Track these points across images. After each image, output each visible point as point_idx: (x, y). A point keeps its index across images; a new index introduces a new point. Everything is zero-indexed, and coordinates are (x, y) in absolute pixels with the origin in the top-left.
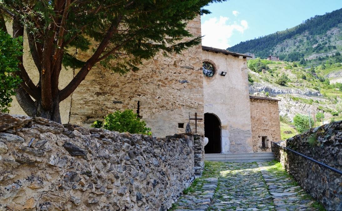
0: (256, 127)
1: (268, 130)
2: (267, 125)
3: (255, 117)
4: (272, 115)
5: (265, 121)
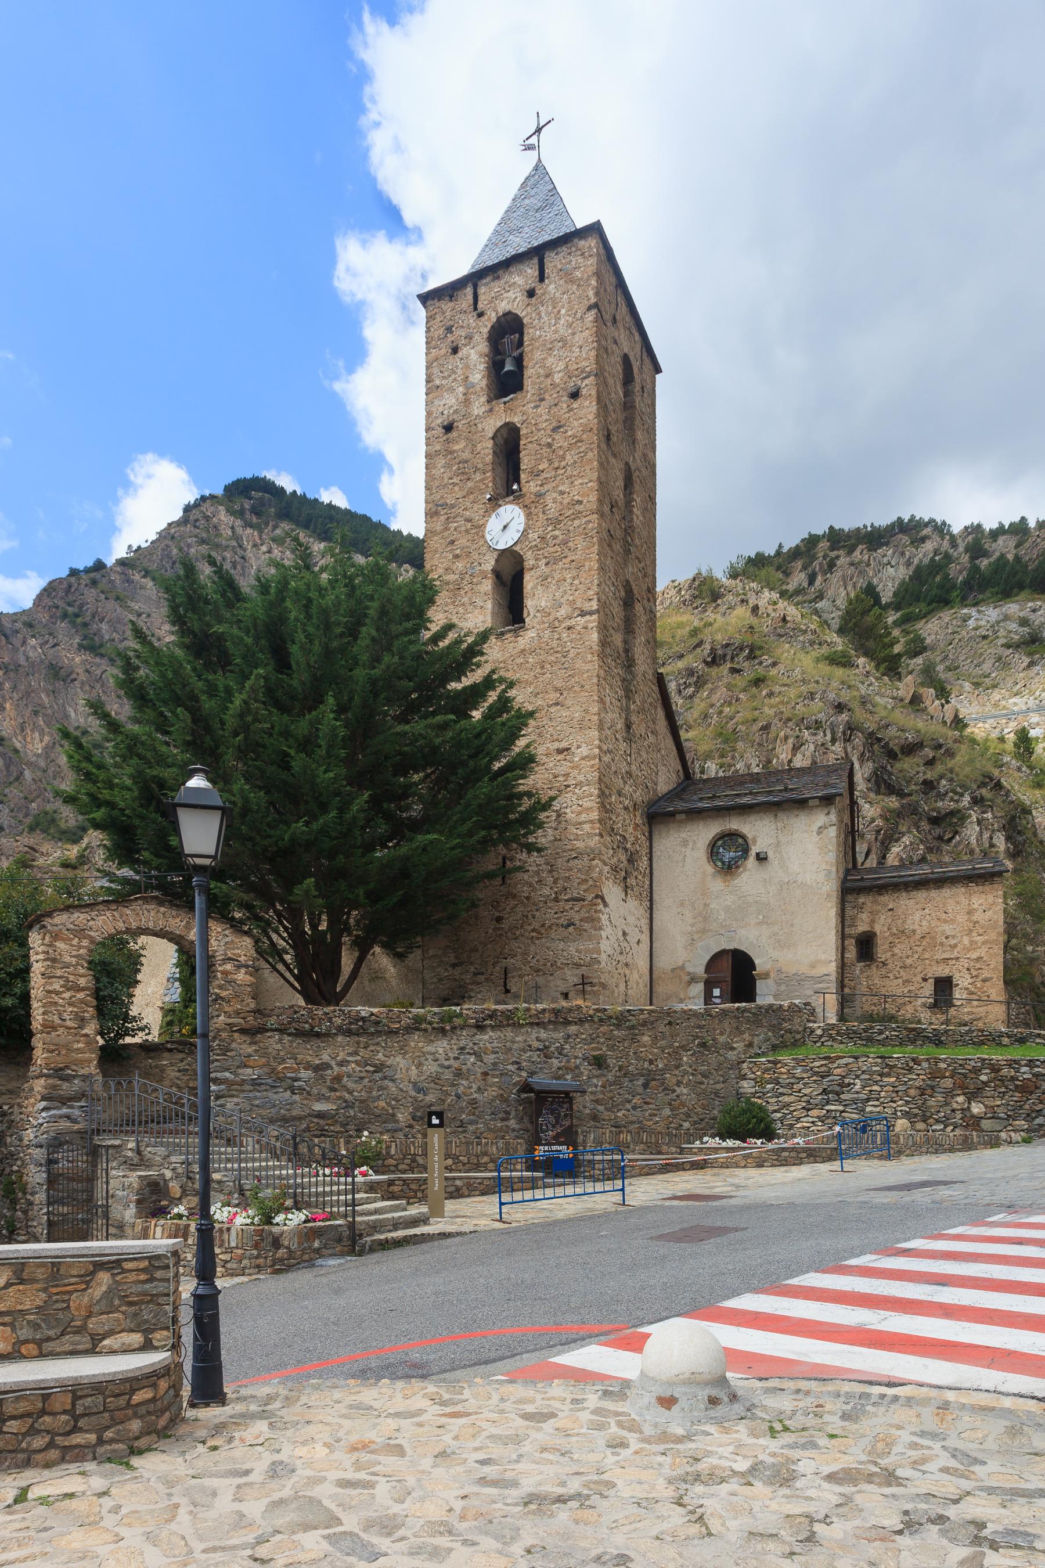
0: (916, 956)
1: (957, 959)
2: (955, 946)
3: (914, 931)
4: (977, 916)
5: (947, 938)
